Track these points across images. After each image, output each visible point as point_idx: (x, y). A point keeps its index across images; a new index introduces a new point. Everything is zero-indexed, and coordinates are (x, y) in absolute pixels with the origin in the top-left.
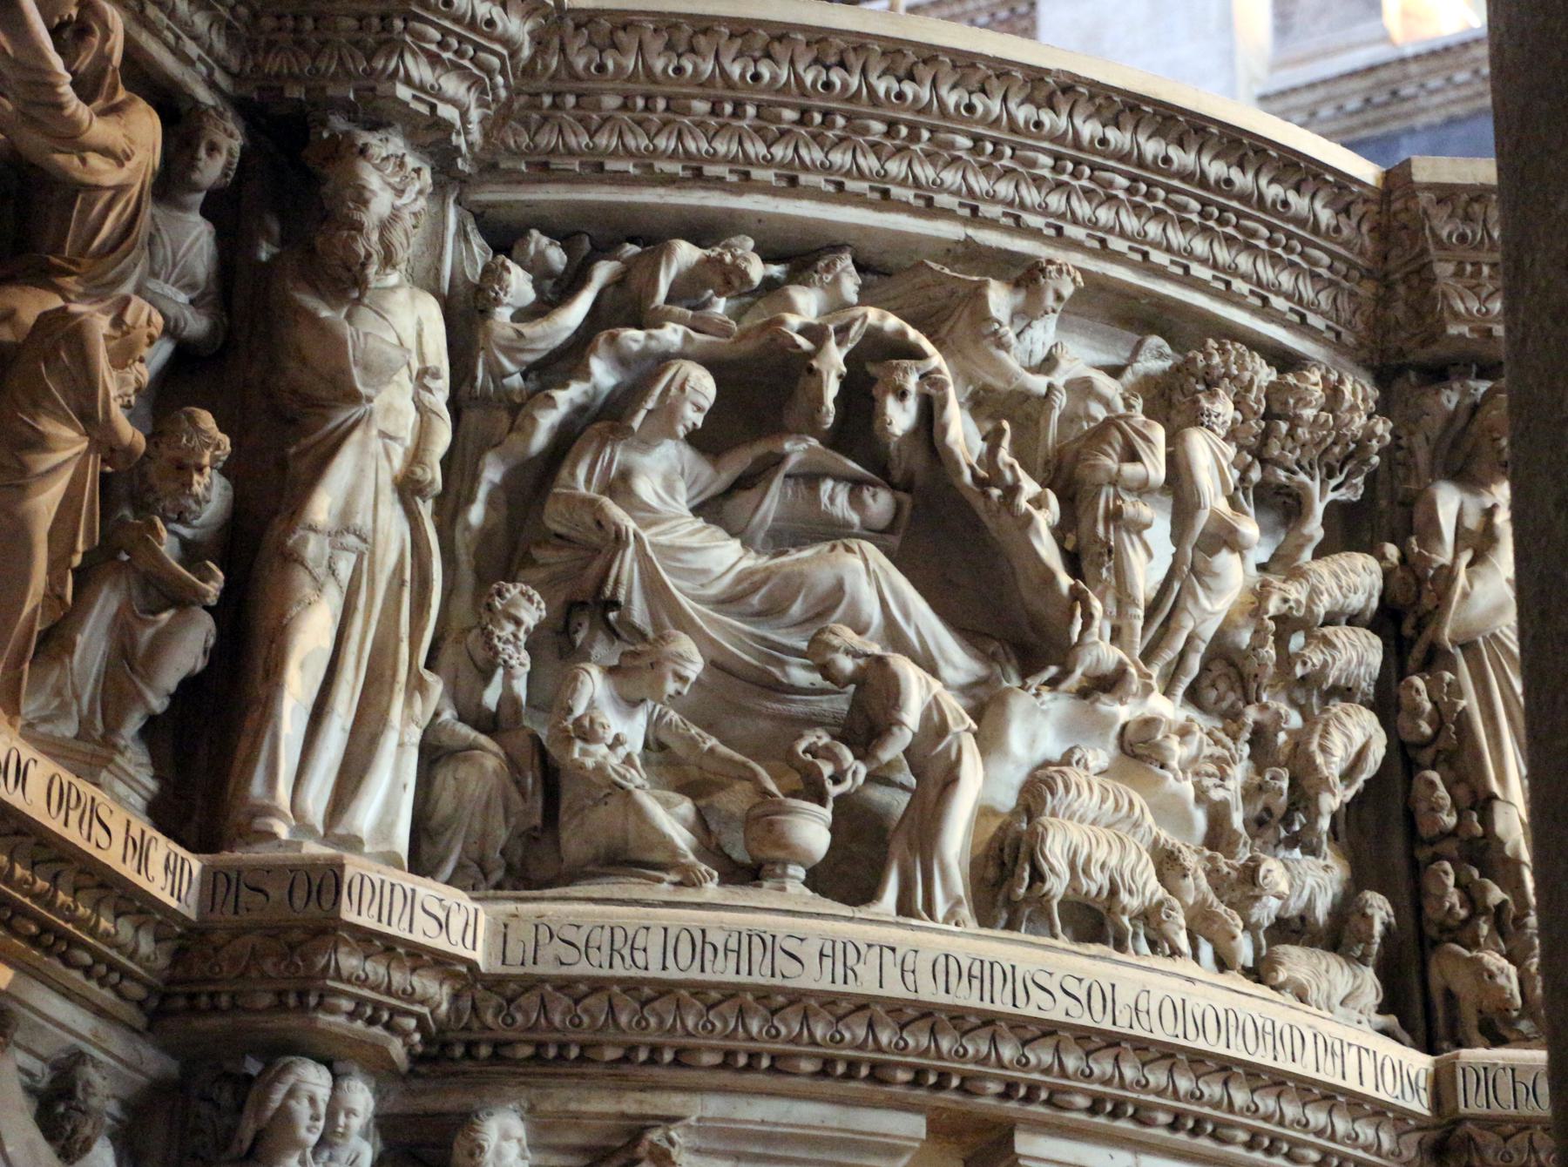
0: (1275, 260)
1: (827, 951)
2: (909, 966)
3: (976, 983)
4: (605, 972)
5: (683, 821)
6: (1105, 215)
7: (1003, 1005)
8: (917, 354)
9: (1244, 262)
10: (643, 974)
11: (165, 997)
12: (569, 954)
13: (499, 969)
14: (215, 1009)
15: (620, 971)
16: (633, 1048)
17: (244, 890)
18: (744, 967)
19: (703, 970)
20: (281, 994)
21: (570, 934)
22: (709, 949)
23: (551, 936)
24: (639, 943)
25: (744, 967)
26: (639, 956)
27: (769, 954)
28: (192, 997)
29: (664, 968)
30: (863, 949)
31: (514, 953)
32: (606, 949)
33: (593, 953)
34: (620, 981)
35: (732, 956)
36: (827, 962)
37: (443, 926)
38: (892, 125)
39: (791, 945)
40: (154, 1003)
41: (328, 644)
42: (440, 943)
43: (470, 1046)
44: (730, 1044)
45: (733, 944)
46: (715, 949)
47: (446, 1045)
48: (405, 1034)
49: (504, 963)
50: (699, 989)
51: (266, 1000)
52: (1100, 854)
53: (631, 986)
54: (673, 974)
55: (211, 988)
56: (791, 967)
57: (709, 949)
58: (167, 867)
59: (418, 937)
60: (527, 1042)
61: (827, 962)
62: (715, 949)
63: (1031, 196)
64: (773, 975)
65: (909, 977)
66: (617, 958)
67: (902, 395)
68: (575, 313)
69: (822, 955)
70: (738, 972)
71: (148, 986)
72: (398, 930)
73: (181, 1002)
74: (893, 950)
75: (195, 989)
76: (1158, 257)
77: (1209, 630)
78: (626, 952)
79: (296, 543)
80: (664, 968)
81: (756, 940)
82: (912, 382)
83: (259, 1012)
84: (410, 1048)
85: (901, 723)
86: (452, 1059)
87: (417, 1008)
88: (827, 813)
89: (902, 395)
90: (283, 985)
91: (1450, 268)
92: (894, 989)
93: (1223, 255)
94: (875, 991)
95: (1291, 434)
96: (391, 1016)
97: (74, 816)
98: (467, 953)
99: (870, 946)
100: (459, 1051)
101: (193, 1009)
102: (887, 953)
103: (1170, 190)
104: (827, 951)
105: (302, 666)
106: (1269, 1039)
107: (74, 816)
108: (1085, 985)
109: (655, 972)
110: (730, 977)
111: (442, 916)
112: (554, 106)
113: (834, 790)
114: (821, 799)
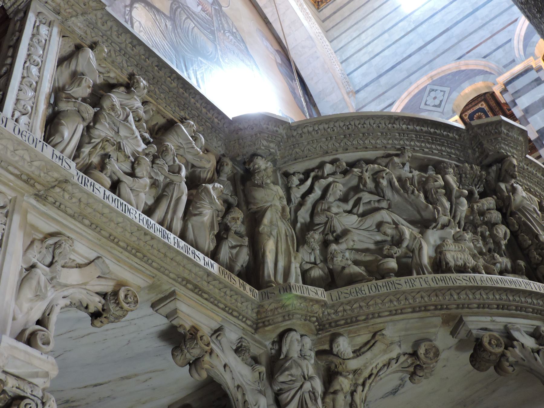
0: (449, 147)
1: (406, 281)
2: (426, 280)
3: (443, 281)
4: (356, 297)
5: (363, 270)
6: (412, 143)
7: (451, 284)
8: (384, 170)
9: (443, 148)
10: (365, 295)
11: (257, 324)
12: (347, 296)
13: (331, 302)
14: (270, 325)
15: (360, 296)
16: (368, 315)
17: (269, 294)
18: (388, 288)
19: (379, 291)
20: (284, 316)
21: (346, 291)
22: (379, 288)
23: (342, 293)
24: (363, 289)
25: (388, 288)
26: (363, 292)
27: (393, 285)
28: (264, 322)
29: (370, 293)
30: (415, 280)
31: (334, 298)
32: (355, 292)
33: (353, 294)
34: (361, 298)
35: (385, 287)
36: (407, 284)
37: (317, 294)
38: (363, 134)
39: (398, 282)
40: (255, 326)
41: (274, 248)
42: (316, 297)
43: (330, 323)
44: (390, 309)
45: (384, 284)
46: (381, 287)
47: (324, 325)
48: (314, 323)
49: (332, 301)
50: (379, 296)
51: (280, 319)
52: (459, 256)
53: (363, 299)
54: (372, 294)
55: (267, 319)
56: (399, 286)
57: (379, 288)
58: (250, 290)
59: (311, 296)
60: (343, 320)
61: (407, 284)
62: (381, 287)
63: (396, 142)
64: (396, 289)
65: (428, 283)
66: (358, 294)
67: (383, 178)
68: (309, 182)
69: (406, 283)
70: (387, 290)
71: (252, 322)
72: (306, 295)
73: (261, 325)
74: (422, 278)
75: (264, 320)
76: (426, 150)
77: (464, 215)
78: (360, 292)
79: (262, 230)
80: (370, 293)
81: (389, 283)
82: (384, 175)
83: (279, 322)
84: (316, 326)
85: (406, 238)
86: (327, 328)
87: (315, 315)
88: (395, 260)
89: (383, 178)
90: (283, 314)
91: (486, 141)
92: (424, 285)
93: (439, 148)
94: (420, 287)
95: (466, 177)
96: (310, 318)
97: (226, 276)
98: (324, 299)
99: (416, 278)
100: (327, 326)
101: (265, 326)
102: (421, 279)
103: (424, 136)
104: (406, 281)
105: (270, 252)
106: (513, 283)
107: (226, 276)
108: (468, 277)
109: (368, 294)
110: (386, 291)
111: (316, 292)
112: (294, 147)
113: (395, 256)
114: (392, 257)
